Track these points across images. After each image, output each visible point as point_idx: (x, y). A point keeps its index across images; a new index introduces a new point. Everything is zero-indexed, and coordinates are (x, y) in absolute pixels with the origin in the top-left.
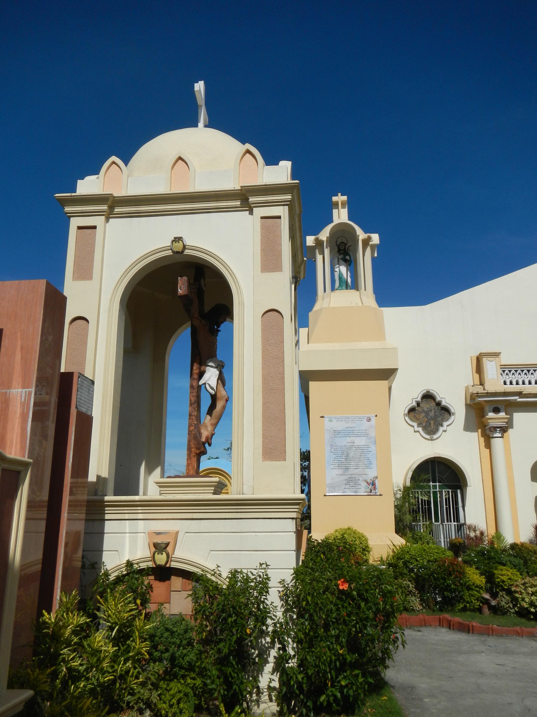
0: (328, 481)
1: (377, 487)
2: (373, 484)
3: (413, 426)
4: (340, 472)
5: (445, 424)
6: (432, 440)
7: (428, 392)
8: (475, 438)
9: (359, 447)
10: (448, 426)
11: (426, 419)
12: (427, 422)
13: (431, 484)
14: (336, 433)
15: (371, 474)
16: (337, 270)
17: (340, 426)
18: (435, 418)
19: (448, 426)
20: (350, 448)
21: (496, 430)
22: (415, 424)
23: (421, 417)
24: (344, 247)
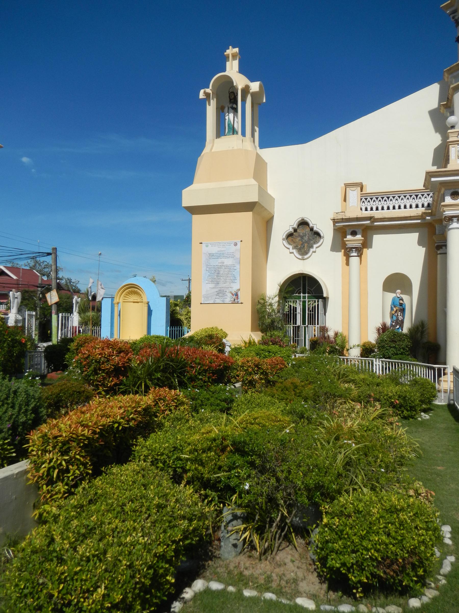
0: (204, 293)
1: (239, 297)
2: (237, 295)
3: (289, 249)
4: (212, 285)
5: (315, 246)
6: (303, 259)
7: (303, 219)
8: (340, 256)
9: (227, 267)
10: (317, 248)
11: (301, 242)
12: (302, 244)
13: (302, 295)
14: (211, 256)
15: (235, 287)
16: (227, 118)
17: (214, 250)
18: (308, 242)
19: (317, 248)
20: (221, 267)
21: (352, 251)
22: (291, 247)
23: (297, 240)
24: (233, 96)
